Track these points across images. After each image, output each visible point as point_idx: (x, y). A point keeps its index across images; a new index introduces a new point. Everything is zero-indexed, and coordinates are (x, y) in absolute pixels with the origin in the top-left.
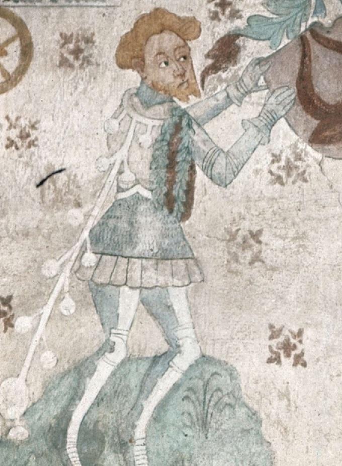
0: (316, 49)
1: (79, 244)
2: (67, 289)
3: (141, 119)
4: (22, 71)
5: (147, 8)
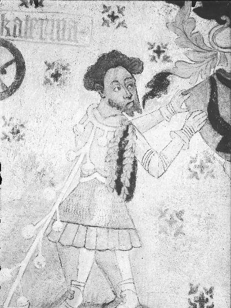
0: (220, 86)
1: (52, 214)
3: (100, 126)
4: (16, 86)
5: (107, 50)
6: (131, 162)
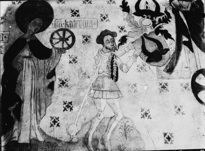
0: (145, 39)
1: (90, 88)
2: (87, 99)
3: (103, 56)
5: (104, 30)
6: (116, 68)
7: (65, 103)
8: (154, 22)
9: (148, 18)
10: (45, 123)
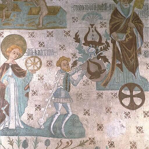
0: (90, 63)
2: (50, 103)
3: (61, 75)
4: (40, 67)
7: (36, 106)
8: (97, 50)
9: (93, 47)
10: (24, 117)
